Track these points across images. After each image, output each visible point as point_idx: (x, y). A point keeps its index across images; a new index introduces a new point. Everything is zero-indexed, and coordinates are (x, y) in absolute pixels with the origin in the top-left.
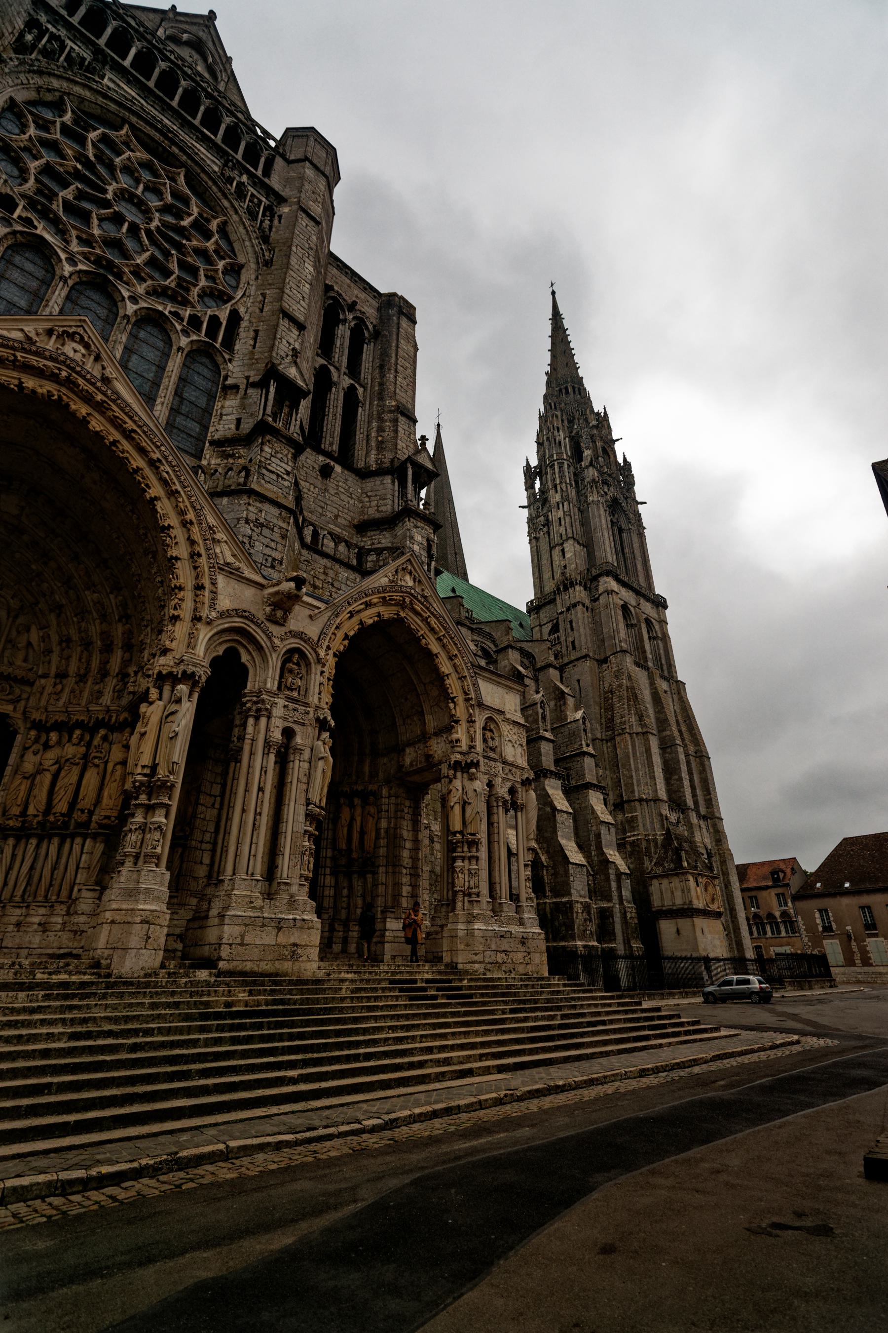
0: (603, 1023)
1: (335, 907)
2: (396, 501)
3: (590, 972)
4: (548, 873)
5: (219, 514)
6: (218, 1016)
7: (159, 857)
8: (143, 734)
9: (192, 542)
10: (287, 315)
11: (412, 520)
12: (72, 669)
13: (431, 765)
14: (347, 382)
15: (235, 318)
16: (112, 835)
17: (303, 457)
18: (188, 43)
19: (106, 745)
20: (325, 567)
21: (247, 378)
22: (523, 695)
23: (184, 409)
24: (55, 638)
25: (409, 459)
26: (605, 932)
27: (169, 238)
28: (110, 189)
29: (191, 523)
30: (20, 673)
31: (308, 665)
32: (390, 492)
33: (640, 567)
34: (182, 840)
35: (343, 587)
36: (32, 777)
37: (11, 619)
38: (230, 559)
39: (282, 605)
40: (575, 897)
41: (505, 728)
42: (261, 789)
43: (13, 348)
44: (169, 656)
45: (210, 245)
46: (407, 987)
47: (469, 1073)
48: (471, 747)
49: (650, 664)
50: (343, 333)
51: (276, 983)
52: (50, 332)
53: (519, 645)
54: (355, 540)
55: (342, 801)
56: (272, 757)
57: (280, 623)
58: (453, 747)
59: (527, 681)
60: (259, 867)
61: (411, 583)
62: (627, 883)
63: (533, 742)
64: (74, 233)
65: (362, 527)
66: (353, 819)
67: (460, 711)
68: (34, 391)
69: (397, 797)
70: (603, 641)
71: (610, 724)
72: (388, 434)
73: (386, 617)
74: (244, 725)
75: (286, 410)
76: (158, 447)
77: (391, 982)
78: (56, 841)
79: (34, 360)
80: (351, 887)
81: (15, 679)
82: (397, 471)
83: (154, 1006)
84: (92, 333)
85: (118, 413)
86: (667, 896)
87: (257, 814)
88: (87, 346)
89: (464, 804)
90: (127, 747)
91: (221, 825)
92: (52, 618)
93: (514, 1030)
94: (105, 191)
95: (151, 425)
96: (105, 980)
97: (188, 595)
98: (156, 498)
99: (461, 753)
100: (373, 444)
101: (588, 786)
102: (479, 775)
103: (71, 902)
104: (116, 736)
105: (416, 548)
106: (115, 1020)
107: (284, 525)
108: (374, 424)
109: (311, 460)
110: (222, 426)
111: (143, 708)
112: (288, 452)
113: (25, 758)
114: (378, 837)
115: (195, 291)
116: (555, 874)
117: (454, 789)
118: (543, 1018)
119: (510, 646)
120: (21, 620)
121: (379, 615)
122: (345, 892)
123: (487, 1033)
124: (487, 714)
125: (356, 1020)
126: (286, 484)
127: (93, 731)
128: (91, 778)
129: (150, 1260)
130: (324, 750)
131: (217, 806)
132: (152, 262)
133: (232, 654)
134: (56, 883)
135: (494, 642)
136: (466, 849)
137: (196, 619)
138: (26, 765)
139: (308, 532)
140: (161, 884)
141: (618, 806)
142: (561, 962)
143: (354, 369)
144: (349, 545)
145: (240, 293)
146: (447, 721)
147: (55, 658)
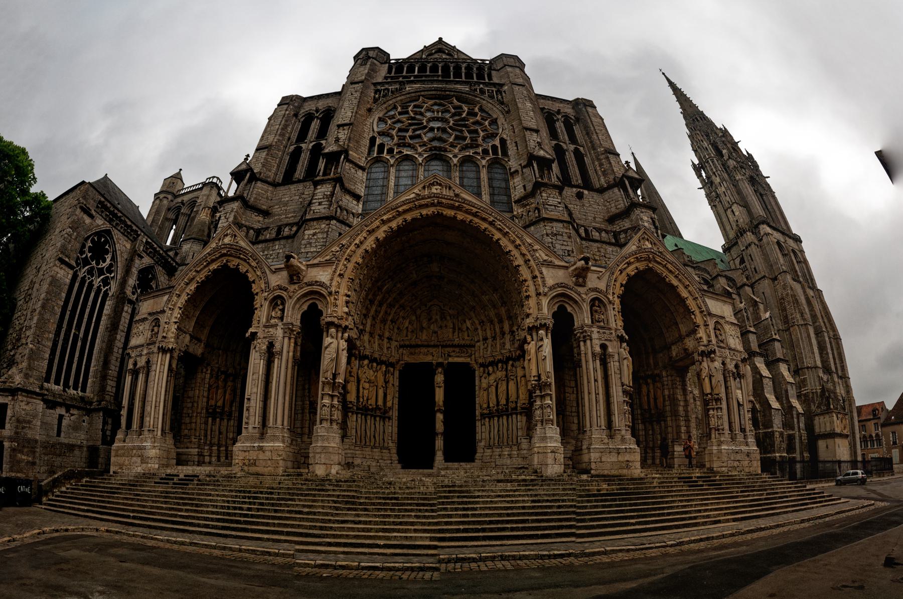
0: (787, 497)
1: (646, 441)
3: (782, 470)
4: (761, 415)
6: (594, 495)
17: (564, 192)
18: (436, 52)
22: (733, 305)
26: (791, 448)
27: (460, 124)
33: (779, 217)
36: (487, 389)
39: (581, 275)
40: (775, 429)
41: (727, 327)
42: (596, 380)
44: (531, 317)
45: (478, 118)
46: (687, 480)
47: (719, 522)
48: (710, 341)
49: (801, 279)
50: (560, 126)
53: (724, 274)
54: (609, 228)
56: (598, 362)
57: (583, 285)
59: (734, 296)
60: (603, 422)
61: (650, 246)
62: (802, 419)
63: (744, 334)
65: (611, 220)
66: (649, 391)
67: (699, 320)
70: (771, 266)
71: (786, 320)
73: (641, 269)
78: (505, 417)
80: (653, 430)
82: (619, 184)
86: (823, 425)
87: (597, 394)
89: (711, 377)
90: (524, 368)
93: (742, 501)
96: (540, 479)
97: (530, 282)
98: (499, 239)
101: (779, 360)
102: (717, 358)
104: (517, 364)
105: (646, 224)
106: (549, 495)
109: (569, 192)
114: (664, 400)
116: (764, 416)
118: (757, 495)
119: (718, 275)
121: (637, 268)
123: (729, 503)
125: (662, 497)
127: (506, 363)
129: (578, 586)
130: (625, 353)
132: (457, 138)
133: (562, 309)
135: (708, 273)
137: (538, 294)
139: (582, 231)
141: (796, 372)
142: (767, 465)
143: (573, 139)
144: (607, 232)
145: (500, 130)
146: (692, 327)
147: (480, 331)
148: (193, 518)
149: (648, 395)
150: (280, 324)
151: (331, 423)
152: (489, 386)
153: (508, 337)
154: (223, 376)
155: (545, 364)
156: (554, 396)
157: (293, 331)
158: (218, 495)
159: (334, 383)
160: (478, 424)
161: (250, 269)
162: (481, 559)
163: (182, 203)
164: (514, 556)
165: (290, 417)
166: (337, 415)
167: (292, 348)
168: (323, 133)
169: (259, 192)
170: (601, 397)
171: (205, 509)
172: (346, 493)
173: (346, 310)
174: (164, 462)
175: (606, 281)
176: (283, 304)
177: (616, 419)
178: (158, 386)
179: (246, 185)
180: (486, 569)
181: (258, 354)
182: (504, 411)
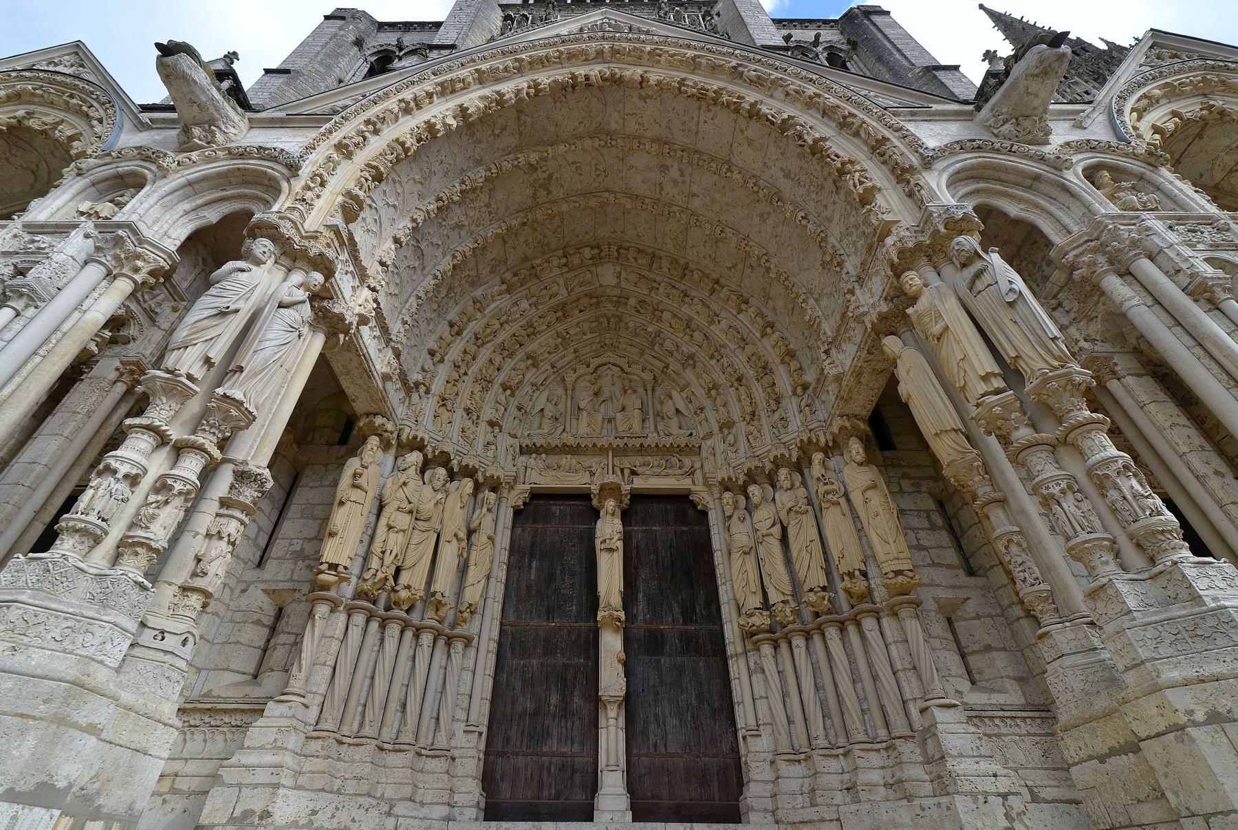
12: (736, 414)
24: (701, 393)
30: (682, 441)
37: (649, 392)
68: (587, 78)
92: (689, 374)
113: (733, 530)
127: (800, 466)
128: (836, 524)
138: (737, 537)
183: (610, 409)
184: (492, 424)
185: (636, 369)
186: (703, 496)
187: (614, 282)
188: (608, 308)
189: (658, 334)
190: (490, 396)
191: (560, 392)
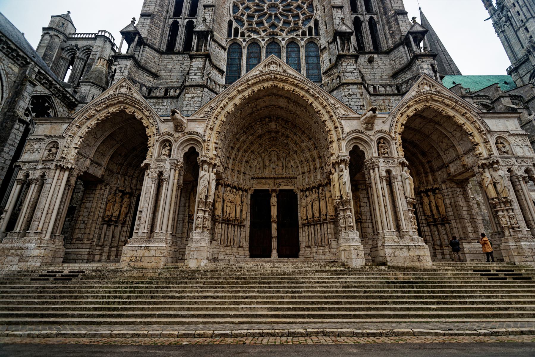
2: (408, 55)
5: (334, 98)
7: (353, 227)
8: (334, 185)
9: (328, 112)
10: (334, 7)
11: (419, 60)
12: (306, 170)
13: (466, 169)
14: (368, 17)
15: (316, 23)
16: (335, 221)
17: (359, 60)
19: (323, 192)
20: (383, 100)
21: (328, 42)
22: (519, 119)
23: (310, 67)
24: (298, 162)
25: (409, 32)
28: (265, 8)
29: (326, 106)
30: (292, 176)
31: (388, 142)
32: (404, 53)
34: (359, 221)
35: (394, 105)
38: (344, 113)
39: (370, 123)
41: (511, 140)
43: (258, 77)
46: (485, 273)
51: (414, 271)
52: (265, 66)
55: (422, 195)
58: (478, 157)
60: (392, 226)
61: (428, 88)
64: (261, 30)
65: (395, 75)
66: (430, 202)
67: (477, 138)
68: (267, 87)
69: (451, 188)
72: (394, 27)
73: (420, 109)
74: (369, 173)
75: (346, 45)
76: (306, 85)
77: (474, 271)
79: (264, 77)
80: (438, 231)
81: (292, 178)
82: (405, 42)
83: (367, 278)
84: (276, 58)
85: (292, 80)
87: (385, 206)
88: (276, 64)
90: (330, 191)
91: (372, 213)
92: (295, 155)
94: (264, 9)
95: (302, 78)
98: (312, 103)
99: (484, 159)
100: (388, 36)
103: (329, 245)
104: (325, 188)
105: (426, 71)
107: (360, 91)
108: (386, 27)
109: (363, 59)
110: (325, 66)
111: (331, 176)
112: (352, 61)
114: (446, 208)
115: (300, 22)
117: (485, 178)
120: (287, 159)
121: (416, 110)
122: (436, 233)
124: (496, 135)
126: (356, 74)
127: (318, 188)
128: (323, 204)
131: (368, 206)
132: (284, 23)
134: (323, 239)
135: (488, 98)
136: (503, 205)
139: (371, 89)
140: (357, 236)
144: (391, 86)
145: (315, 11)
148: (69, 309)
149: (430, 204)
150: (168, 159)
151: (203, 229)
152: (307, 205)
153: (318, 171)
154: (121, 194)
155: (345, 187)
156: (353, 209)
157: (177, 165)
158: (100, 287)
159: (206, 202)
160: (300, 230)
161: (144, 117)
162: (307, 334)
163: (76, 46)
164: (333, 333)
165: (173, 225)
166: (208, 224)
167: (177, 177)
168: (193, 12)
169: (146, 55)
170: (389, 208)
171: (84, 300)
172: (210, 281)
173: (215, 153)
174: (49, 260)
175: (391, 123)
176: (170, 145)
177: (405, 224)
178: (54, 195)
179: (136, 47)
180: (311, 343)
181: (150, 179)
182: (319, 222)
183: (273, 165)
184: (243, 173)
185: (281, 152)
186: (297, 192)
187: (275, 127)
188: (273, 134)
189: (287, 143)
190: (243, 165)
191: (260, 159)
